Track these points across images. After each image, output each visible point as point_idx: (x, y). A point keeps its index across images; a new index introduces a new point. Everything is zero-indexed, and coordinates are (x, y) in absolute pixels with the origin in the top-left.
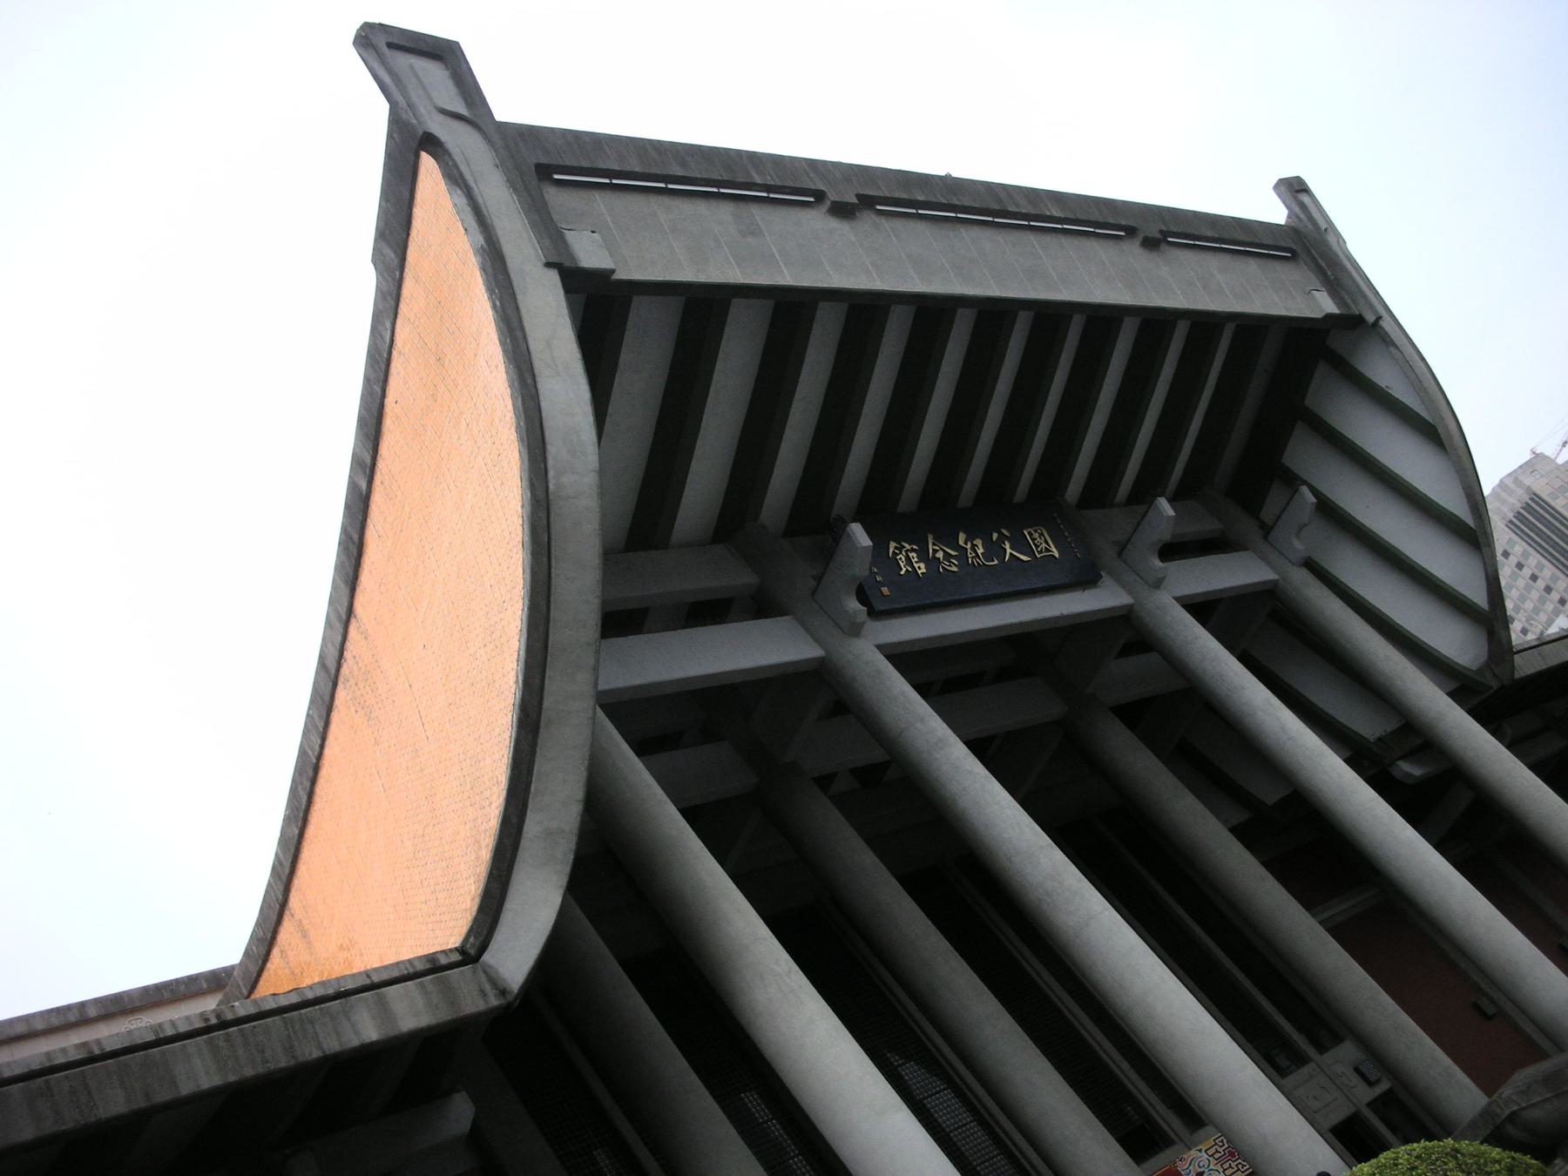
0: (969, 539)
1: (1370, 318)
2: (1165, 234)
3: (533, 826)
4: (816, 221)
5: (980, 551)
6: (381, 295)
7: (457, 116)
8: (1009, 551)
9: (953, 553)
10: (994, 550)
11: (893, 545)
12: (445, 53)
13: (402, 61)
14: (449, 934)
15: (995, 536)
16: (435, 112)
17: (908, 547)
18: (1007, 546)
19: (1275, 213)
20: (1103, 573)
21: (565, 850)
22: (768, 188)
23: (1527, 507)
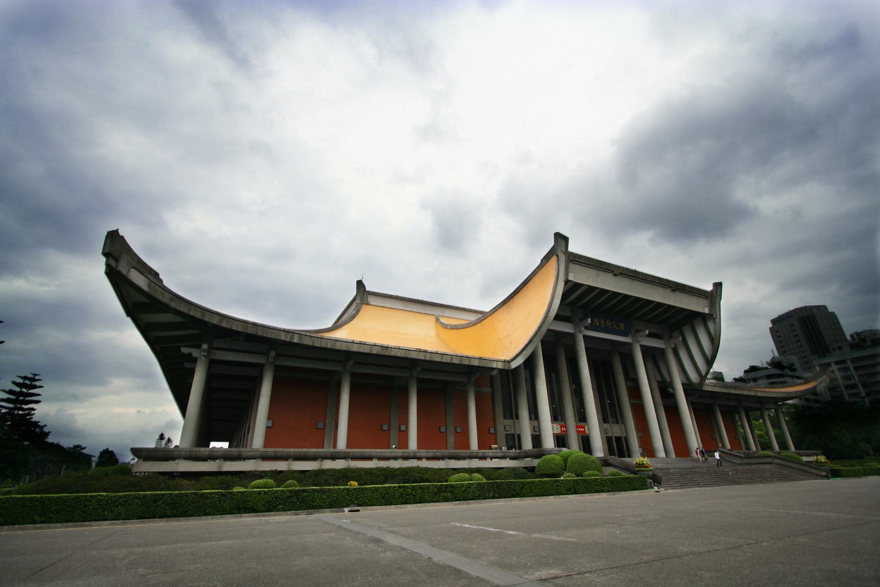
1: (714, 317)
3: (524, 352)
6: (538, 266)
10: (612, 325)
11: (595, 319)
12: (566, 239)
13: (559, 240)
14: (508, 359)
18: (615, 326)
20: (630, 335)
21: (526, 357)
22: (604, 269)
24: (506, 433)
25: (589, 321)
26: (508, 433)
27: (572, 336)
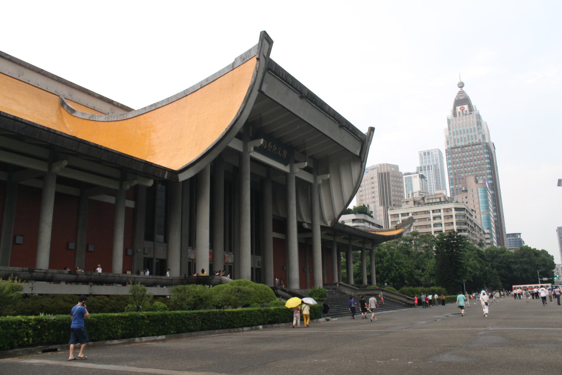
0: (275, 147)
1: (362, 160)
2: (344, 126)
3: (198, 165)
4: (296, 96)
5: (275, 150)
7: (264, 56)
8: (279, 152)
9: (271, 147)
13: (265, 42)
15: (279, 149)
16: (262, 55)
17: (266, 142)
18: (280, 151)
19: (364, 130)
20: (289, 165)
21: (199, 170)
23: (385, 174)
24: (144, 256)
25: (262, 141)
26: (147, 256)
27: (239, 155)
